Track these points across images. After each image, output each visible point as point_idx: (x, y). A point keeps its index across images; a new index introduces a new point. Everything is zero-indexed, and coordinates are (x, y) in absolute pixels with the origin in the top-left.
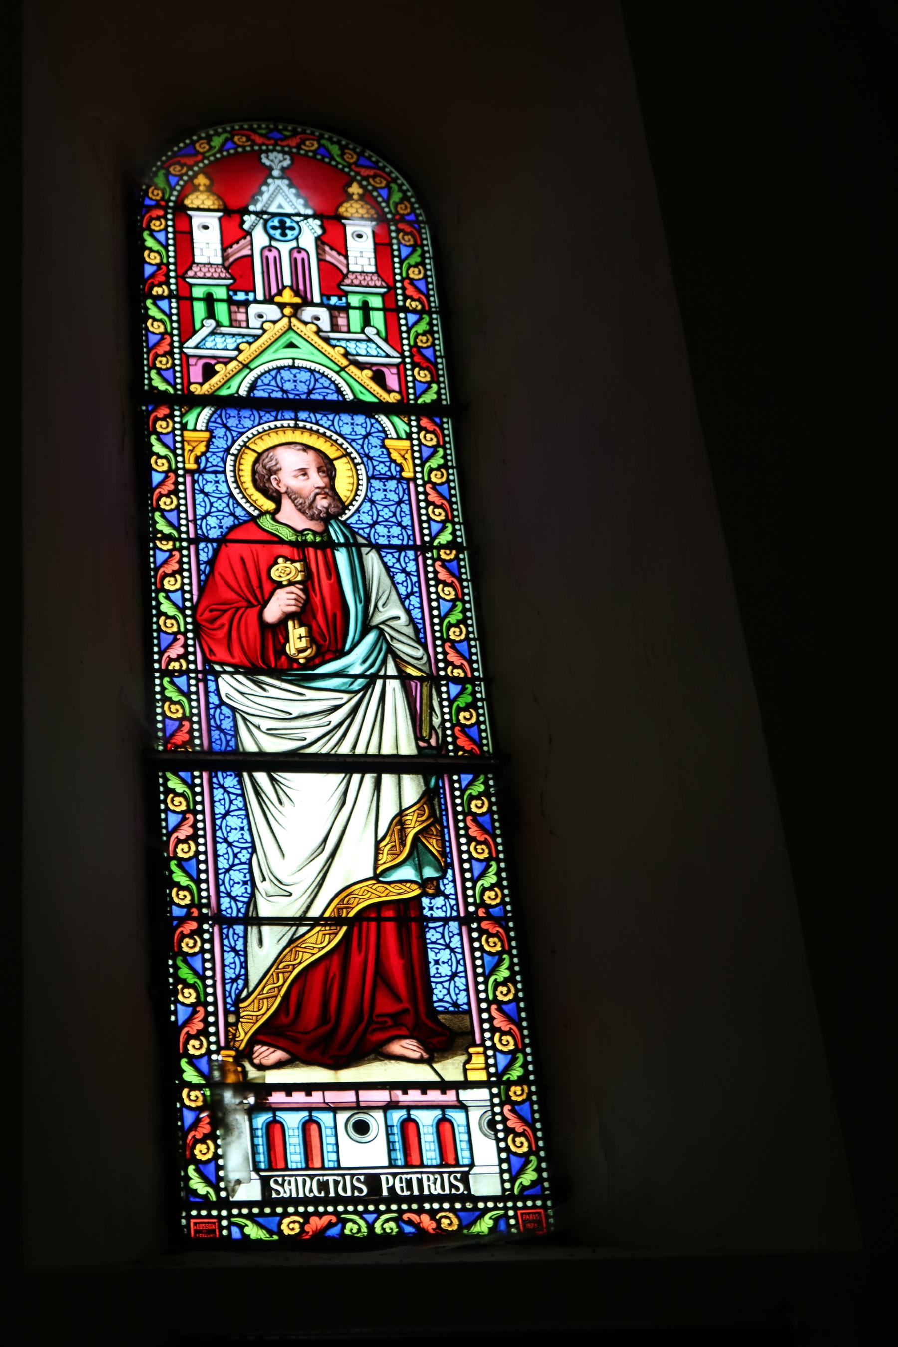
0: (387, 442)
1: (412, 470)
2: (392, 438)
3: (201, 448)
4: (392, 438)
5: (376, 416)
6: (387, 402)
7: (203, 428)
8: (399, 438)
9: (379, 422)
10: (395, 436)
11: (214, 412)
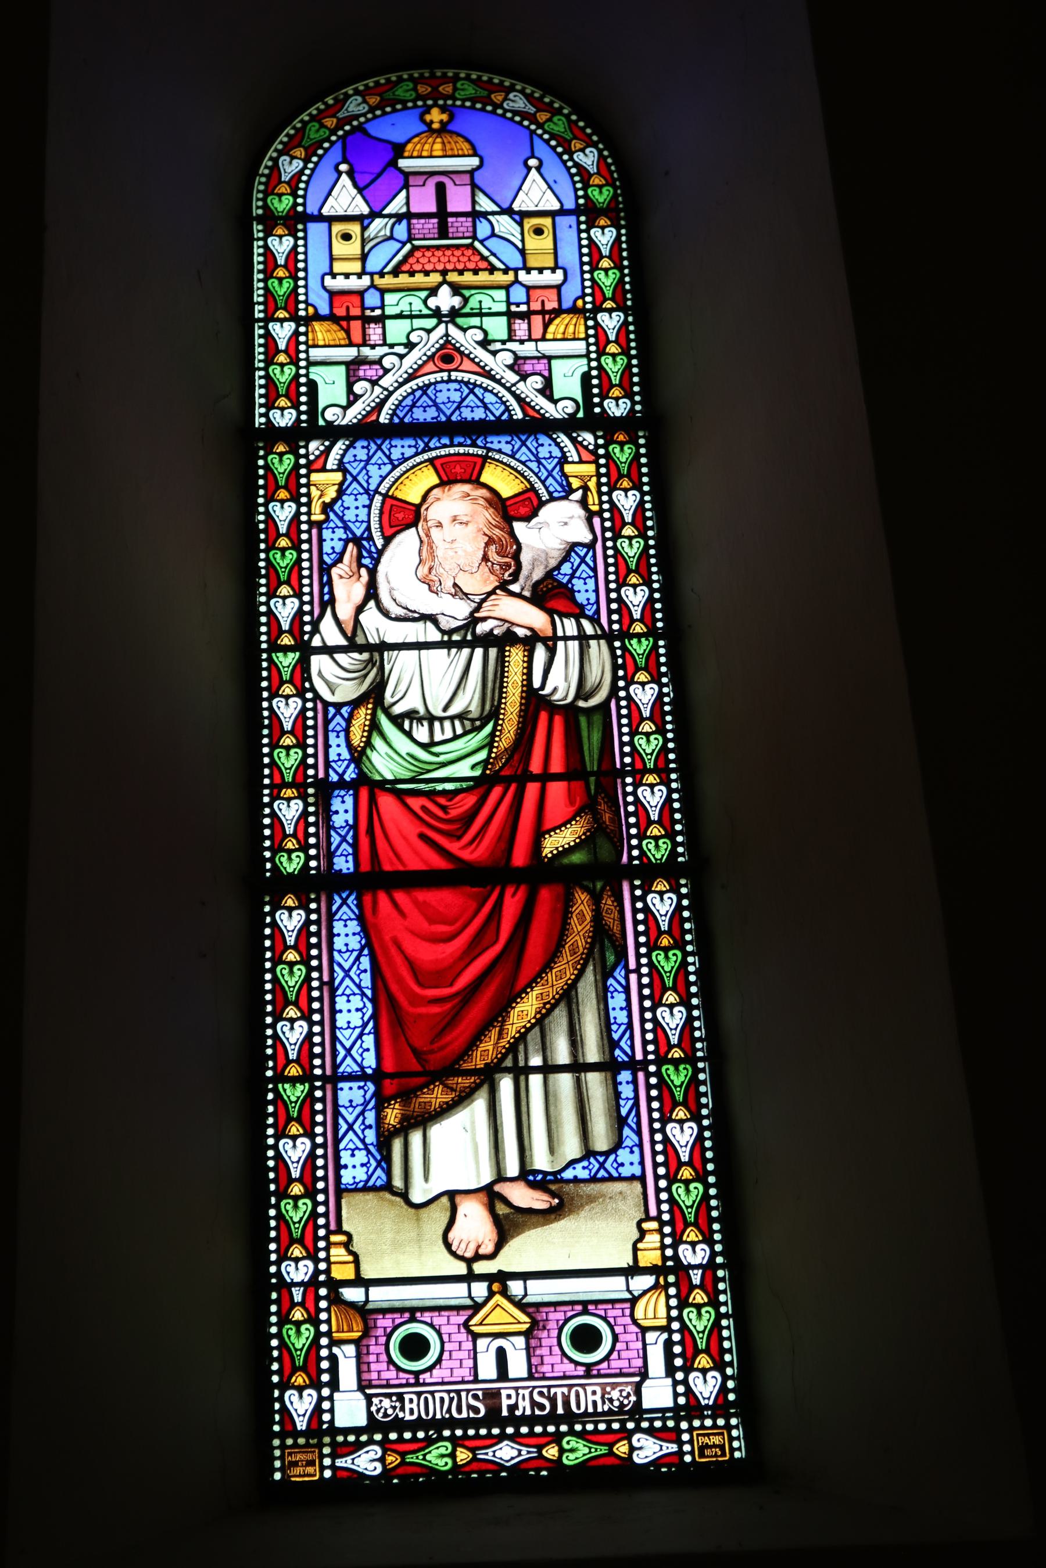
0: (568, 468)
1: (597, 502)
2: (573, 462)
3: (331, 493)
4: (573, 462)
5: (555, 436)
6: (555, 419)
7: (335, 467)
8: (581, 462)
9: (557, 444)
10: (576, 459)
11: (348, 448)
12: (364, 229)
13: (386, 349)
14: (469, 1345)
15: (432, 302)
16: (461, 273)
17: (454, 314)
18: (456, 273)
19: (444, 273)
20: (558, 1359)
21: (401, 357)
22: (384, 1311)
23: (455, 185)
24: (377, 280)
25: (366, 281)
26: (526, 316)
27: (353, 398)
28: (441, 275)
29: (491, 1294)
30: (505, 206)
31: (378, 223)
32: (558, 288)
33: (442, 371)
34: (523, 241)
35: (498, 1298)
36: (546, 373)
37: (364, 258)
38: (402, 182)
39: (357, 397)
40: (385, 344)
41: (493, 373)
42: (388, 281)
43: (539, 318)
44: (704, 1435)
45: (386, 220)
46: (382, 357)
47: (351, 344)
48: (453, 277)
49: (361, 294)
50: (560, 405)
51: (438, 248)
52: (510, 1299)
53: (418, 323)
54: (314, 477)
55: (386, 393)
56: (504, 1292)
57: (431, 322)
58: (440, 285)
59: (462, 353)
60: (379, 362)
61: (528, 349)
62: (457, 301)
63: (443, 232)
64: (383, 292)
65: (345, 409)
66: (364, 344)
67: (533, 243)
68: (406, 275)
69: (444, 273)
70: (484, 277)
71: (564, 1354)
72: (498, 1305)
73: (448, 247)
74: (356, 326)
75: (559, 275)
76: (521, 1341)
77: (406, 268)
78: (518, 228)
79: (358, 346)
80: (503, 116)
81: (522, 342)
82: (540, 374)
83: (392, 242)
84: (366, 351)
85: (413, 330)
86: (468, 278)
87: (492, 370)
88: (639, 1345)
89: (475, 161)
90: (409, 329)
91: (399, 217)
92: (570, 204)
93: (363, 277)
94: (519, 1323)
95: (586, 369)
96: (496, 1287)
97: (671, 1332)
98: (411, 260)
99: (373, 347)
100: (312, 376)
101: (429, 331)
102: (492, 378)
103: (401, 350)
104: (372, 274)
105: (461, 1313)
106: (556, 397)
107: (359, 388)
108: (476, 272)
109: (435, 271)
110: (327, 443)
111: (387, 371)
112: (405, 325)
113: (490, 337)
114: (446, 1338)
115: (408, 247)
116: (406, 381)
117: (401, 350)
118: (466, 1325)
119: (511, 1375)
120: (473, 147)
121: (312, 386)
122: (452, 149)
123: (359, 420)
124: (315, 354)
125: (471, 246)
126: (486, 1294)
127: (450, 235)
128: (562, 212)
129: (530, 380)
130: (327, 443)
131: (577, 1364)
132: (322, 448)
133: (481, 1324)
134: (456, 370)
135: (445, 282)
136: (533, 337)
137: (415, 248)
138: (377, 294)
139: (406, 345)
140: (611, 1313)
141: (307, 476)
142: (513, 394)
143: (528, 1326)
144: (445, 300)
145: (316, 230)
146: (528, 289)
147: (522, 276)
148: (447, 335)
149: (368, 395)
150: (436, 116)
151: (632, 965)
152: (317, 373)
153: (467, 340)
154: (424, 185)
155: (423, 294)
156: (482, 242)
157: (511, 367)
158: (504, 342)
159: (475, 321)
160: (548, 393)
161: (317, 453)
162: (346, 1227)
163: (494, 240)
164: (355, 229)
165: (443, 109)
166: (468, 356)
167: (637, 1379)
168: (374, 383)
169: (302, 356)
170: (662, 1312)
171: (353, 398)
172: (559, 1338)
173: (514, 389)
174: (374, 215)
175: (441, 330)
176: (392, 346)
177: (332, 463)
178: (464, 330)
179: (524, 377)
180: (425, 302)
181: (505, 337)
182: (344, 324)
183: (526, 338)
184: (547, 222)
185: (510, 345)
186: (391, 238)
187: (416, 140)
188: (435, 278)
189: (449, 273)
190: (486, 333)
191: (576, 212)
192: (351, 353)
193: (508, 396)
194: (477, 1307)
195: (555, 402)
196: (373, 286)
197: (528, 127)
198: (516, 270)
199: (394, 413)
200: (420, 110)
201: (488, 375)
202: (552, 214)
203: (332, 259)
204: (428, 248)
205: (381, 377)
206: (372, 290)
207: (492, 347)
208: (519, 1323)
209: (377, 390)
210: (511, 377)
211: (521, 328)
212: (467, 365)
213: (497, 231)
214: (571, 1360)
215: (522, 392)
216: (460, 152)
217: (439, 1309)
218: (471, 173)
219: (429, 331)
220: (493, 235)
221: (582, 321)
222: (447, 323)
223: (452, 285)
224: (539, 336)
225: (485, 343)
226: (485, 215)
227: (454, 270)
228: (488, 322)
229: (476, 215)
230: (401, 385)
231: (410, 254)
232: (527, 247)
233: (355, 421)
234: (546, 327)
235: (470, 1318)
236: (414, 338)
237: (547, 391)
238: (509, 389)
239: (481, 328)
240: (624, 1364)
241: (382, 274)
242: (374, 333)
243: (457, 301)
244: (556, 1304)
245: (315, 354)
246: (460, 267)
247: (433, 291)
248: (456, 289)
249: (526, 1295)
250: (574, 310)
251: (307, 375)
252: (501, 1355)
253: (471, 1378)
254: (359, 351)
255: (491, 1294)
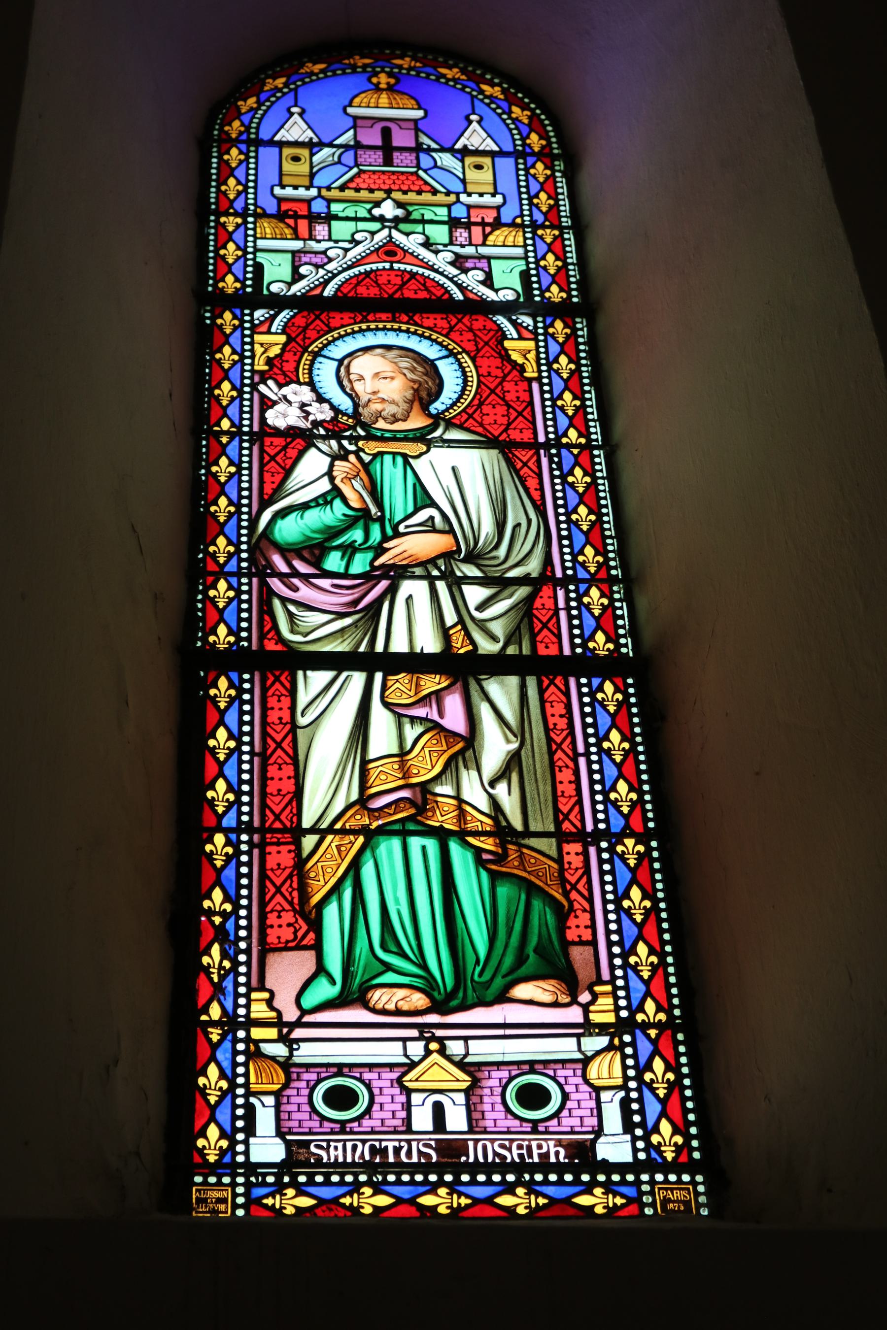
0: (507, 344)
2: (512, 339)
4: (512, 339)
8: (521, 338)
10: (515, 336)
12: (312, 155)
13: (331, 244)
14: (403, 1098)
15: (376, 212)
16: (405, 193)
17: (396, 220)
18: (400, 193)
19: (388, 192)
20: (502, 1115)
21: (346, 250)
22: (308, 1066)
23: (401, 128)
24: (324, 192)
25: (313, 192)
26: (468, 226)
27: (297, 277)
28: (385, 193)
29: (428, 1053)
30: (448, 145)
31: (327, 151)
32: (498, 208)
33: (385, 261)
34: (464, 173)
35: (436, 1057)
36: (487, 269)
37: (312, 176)
38: (351, 124)
39: (302, 277)
40: (330, 239)
41: (436, 267)
42: (335, 193)
43: (480, 228)
44: (666, 1189)
45: (334, 150)
46: (327, 249)
47: (297, 238)
48: (397, 195)
49: (309, 202)
50: (501, 293)
51: (383, 172)
52: (449, 1058)
53: (362, 225)
54: (257, 338)
55: (330, 275)
56: (442, 1051)
57: (376, 226)
58: (384, 200)
59: (402, 249)
60: (324, 252)
61: (470, 250)
62: (400, 212)
63: (388, 161)
64: (329, 201)
65: (290, 285)
66: (311, 238)
67: (472, 175)
68: (353, 191)
69: (388, 192)
70: (427, 197)
71: (508, 1110)
72: (436, 1063)
73: (393, 173)
74: (303, 225)
75: (499, 199)
76: (460, 1098)
77: (353, 185)
78: (460, 164)
79: (304, 240)
80: (446, 83)
81: (463, 246)
82: (482, 270)
83: (339, 166)
84: (312, 244)
85: (357, 232)
86: (412, 197)
87: (434, 264)
88: (593, 1104)
89: (420, 113)
90: (354, 230)
91: (346, 147)
92: (509, 148)
93: (311, 189)
94: (458, 1080)
95: (524, 268)
96: (434, 1046)
97: (628, 1090)
98: (357, 180)
99: (319, 241)
100: (258, 260)
101: (373, 233)
102: (436, 271)
103: (347, 245)
104: (319, 188)
105: (396, 1070)
106: (496, 287)
107: (303, 270)
108: (419, 193)
109: (379, 189)
110: (272, 312)
111: (330, 260)
112: (351, 226)
113: (431, 241)
114: (376, 1091)
115: (355, 170)
116: (350, 267)
117: (347, 245)
118: (399, 1081)
119: (448, 1129)
120: (418, 103)
121: (259, 269)
122: (398, 104)
123: (303, 294)
124: (261, 243)
125: (416, 173)
126: (423, 1053)
127: (395, 164)
128: (502, 153)
129: (470, 273)
130: (272, 312)
131: (522, 1120)
132: (267, 315)
133: (417, 1080)
134: (398, 262)
135: (389, 197)
136: (474, 242)
137: (361, 172)
138: (325, 203)
139: (350, 242)
140: (560, 1073)
141: (251, 336)
142: (455, 283)
143: (469, 1083)
144: (388, 210)
145: (268, 154)
146: (469, 207)
147: (463, 198)
148: (390, 236)
149: (311, 276)
150: (383, 79)
151: (581, 749)
152: (261, 258)
153: (412, 243)
154: (372, 127)
155: (369, 206)
156: (425, 171)
157: (452, 263)
158: (445, 245)
159: (419, 228)
160: (489, 283)
161: (262, 319)
162: (268, 985)
163: (436, 170)
164: (305, 153)
165: (390, 75)
166: (412, 254)
167: (592, 1136)
168: (317, 266)
169: (250, 244)
170: (617, 1071)
171: (297, 277)
172: (503, 1095)
173: (455, 279)
174: (321, 145)
175: (386, 232)
176: (336, 242)
177: (277, 325)
178: (407, 234)
179: (465, 271)
180: (370, 211)
181: (447, 241)
182: (291, 222)
183: (467, 243)
184: (487, 161)
185: (449, 248)
186: (339, 162)
187: (363, 95)
188: (379, 195)
189: (393, 192)
190: (428, 238)
191: (516, 155)
192: (298, 245)
193: (448, 284)
194: (413, 1065)
195: (497, 291)
196: (320, 196)
197: (470, 93)
198: (458, 194)
199: (338, 290)
200: (367, 75)
201: (432, 268)
202: (492, 154)
203: (281, 175)
204: (374, 172)
205: (326, 264)
206: (319, 200)
207: (434, 247)
208: (458, 1080)
209: (322, 272)
210: (453, 271)
211: (461, 235)
212: (408, 258)
213: (439, 164)
214: (516, 1117)
215: (463, 282)
216: (405, 106)
217: (371, 1066)
218: (416, 121)
219: (373, 233)
220: (435, 166)
221: (521, 234)
222: (390, 228)
223: (394, 200)
224: (480, 242)
225: (427, 244)
226: (429, 150)
227: (399, 190)
228: (430, 229)
229: (418, 149)
230: (345, 270)
231: (358, 175)
232: (467, 177)
233: (299, 294)
234: (485, 236)
235: (404, 1074)
236: (358, 237)
237: (488, 281)
238: (451, 280)
239: (423, 234)
240: (576, 1122)
241: (329, 188)
242: (321, 230)
243: (400, 212)
244: (499, 1065)
245: (261, 243)
246: (405, 188)
247: (377, 204)
248: (399, 205)
249: (467, 1054)
250: (513, 225)
251: (254, 259)
252: (439, 1111)
253: (404, 1129)
254: (305, 244)
255: (428, 1053)
